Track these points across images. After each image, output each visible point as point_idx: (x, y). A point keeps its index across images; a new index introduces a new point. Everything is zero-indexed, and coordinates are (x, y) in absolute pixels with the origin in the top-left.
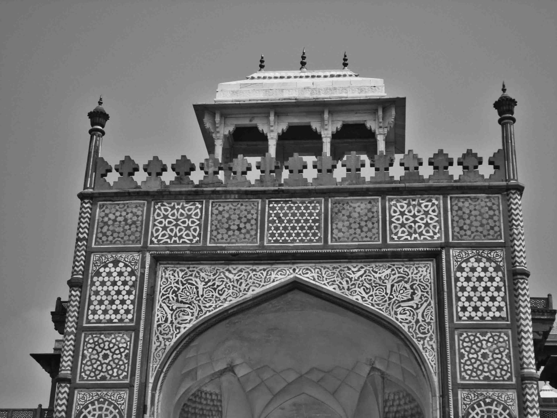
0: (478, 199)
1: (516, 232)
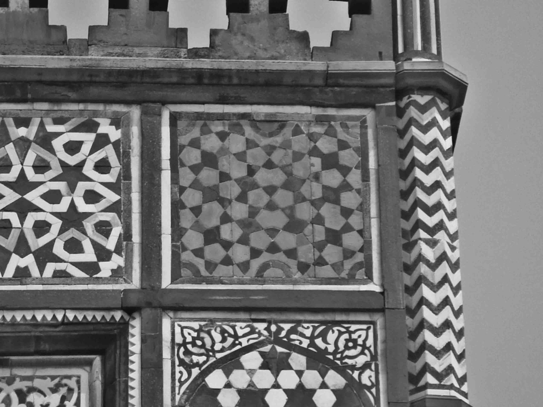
0: (282, 125)
1: (430, 254)
